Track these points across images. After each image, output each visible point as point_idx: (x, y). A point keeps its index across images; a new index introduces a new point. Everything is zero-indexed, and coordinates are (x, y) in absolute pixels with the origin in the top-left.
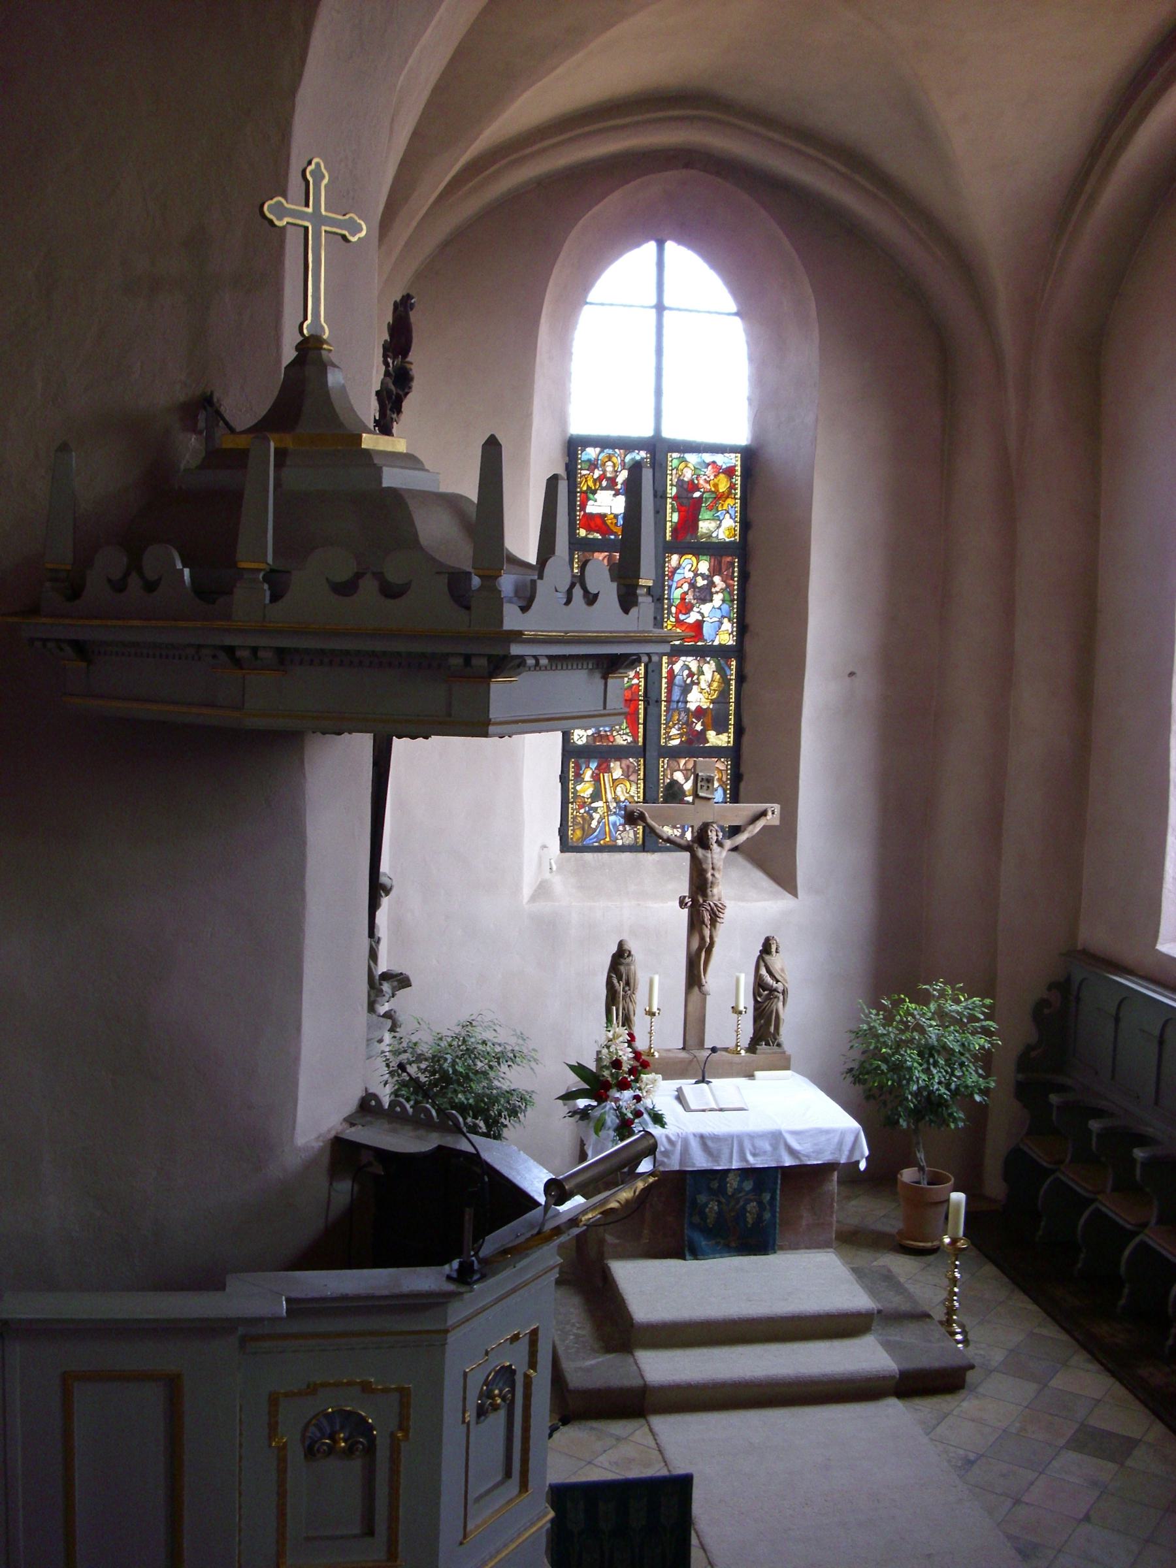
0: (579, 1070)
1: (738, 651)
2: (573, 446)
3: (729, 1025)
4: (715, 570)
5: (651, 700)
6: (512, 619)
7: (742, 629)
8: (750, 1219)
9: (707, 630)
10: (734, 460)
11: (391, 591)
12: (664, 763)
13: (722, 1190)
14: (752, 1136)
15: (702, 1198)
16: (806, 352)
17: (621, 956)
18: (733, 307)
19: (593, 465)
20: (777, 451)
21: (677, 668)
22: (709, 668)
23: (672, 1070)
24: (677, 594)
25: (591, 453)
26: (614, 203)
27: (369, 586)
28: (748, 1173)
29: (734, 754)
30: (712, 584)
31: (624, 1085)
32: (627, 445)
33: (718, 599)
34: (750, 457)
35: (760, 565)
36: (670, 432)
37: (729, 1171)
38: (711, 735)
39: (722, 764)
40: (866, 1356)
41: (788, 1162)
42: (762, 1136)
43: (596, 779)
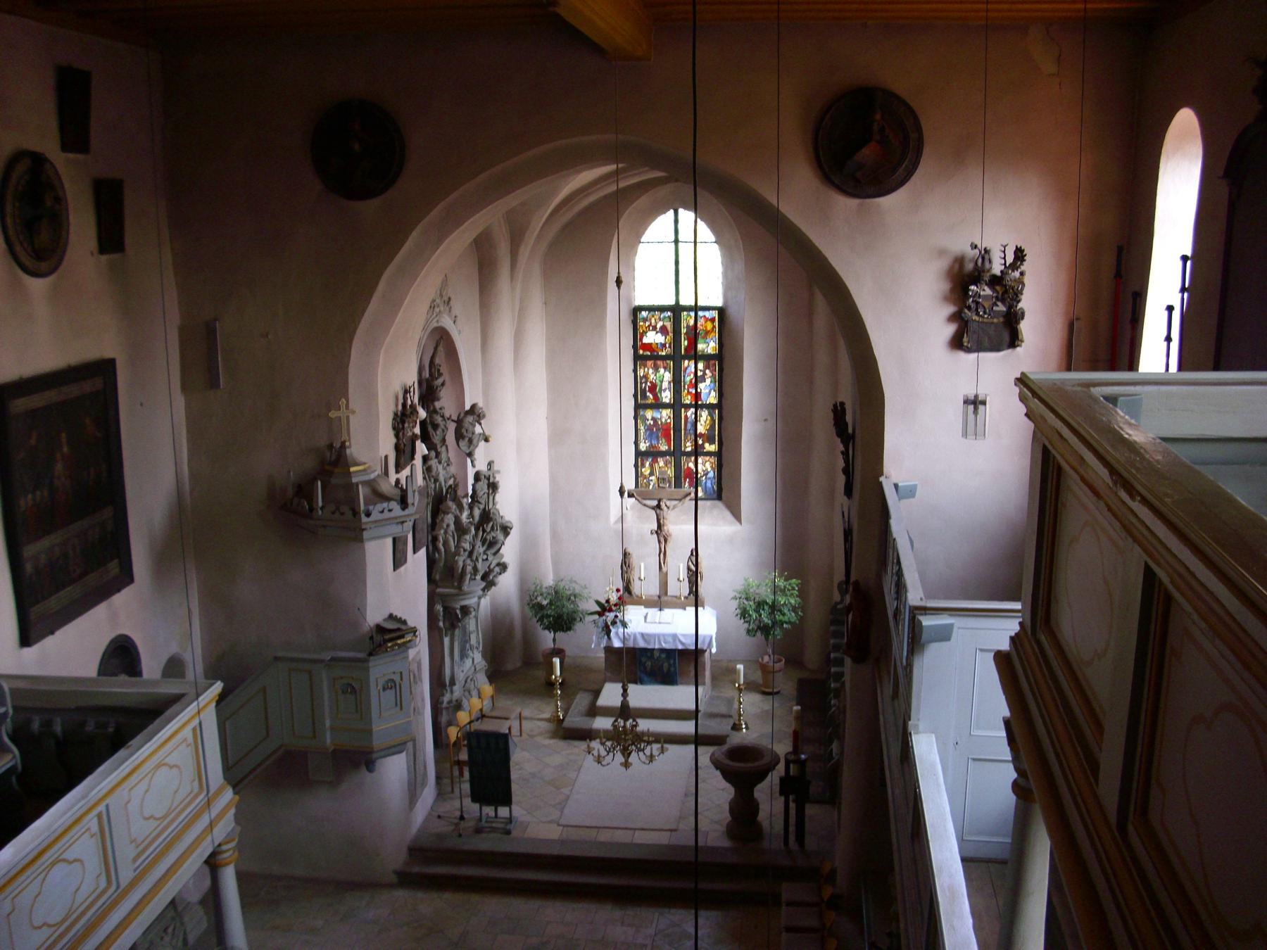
0: (598, 603)
1: (719, 406)
2: (636, 310)
3: (679, 587)
4: (706, 367)
5: (677, 429)
6: (364, 519)
7: (721, 395)
8: (665, 670)
9: (703, 396)
10: (715, 314)
11: (342, 514)
12: (684, 458)
13: (652, 657)
14: (664, 635)
15: (643, 659)
16: (740, 267)
17: (626, 555)
18: (713, 239)
19: (645, 320)
20: (732, 312)
21: (689, 414)
22: (704, 414)
23: (649, 604)
24: (688, 379)
25: (644, 314)
26: (643, 201)
27: (337, 514)
28: (662, 650)
29: (719, 455)
30: (705, 374)
31: (610, 610)
32: (662, 309)
33: (708, 381)
34: (722, 311)
35: (725, 363)
36: (683, 302)
37: (653, 650)
38: (707, 445)
39: (713, 459)
40: (687, 727)
41: (680, 647)
42: (669, 635)
43: (651, 466)
